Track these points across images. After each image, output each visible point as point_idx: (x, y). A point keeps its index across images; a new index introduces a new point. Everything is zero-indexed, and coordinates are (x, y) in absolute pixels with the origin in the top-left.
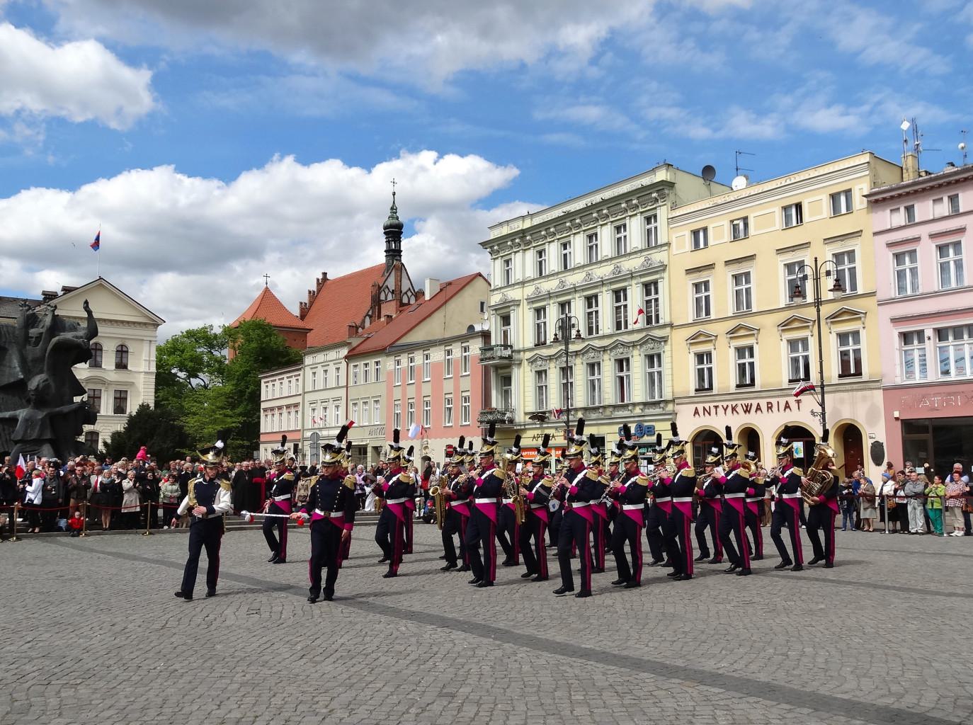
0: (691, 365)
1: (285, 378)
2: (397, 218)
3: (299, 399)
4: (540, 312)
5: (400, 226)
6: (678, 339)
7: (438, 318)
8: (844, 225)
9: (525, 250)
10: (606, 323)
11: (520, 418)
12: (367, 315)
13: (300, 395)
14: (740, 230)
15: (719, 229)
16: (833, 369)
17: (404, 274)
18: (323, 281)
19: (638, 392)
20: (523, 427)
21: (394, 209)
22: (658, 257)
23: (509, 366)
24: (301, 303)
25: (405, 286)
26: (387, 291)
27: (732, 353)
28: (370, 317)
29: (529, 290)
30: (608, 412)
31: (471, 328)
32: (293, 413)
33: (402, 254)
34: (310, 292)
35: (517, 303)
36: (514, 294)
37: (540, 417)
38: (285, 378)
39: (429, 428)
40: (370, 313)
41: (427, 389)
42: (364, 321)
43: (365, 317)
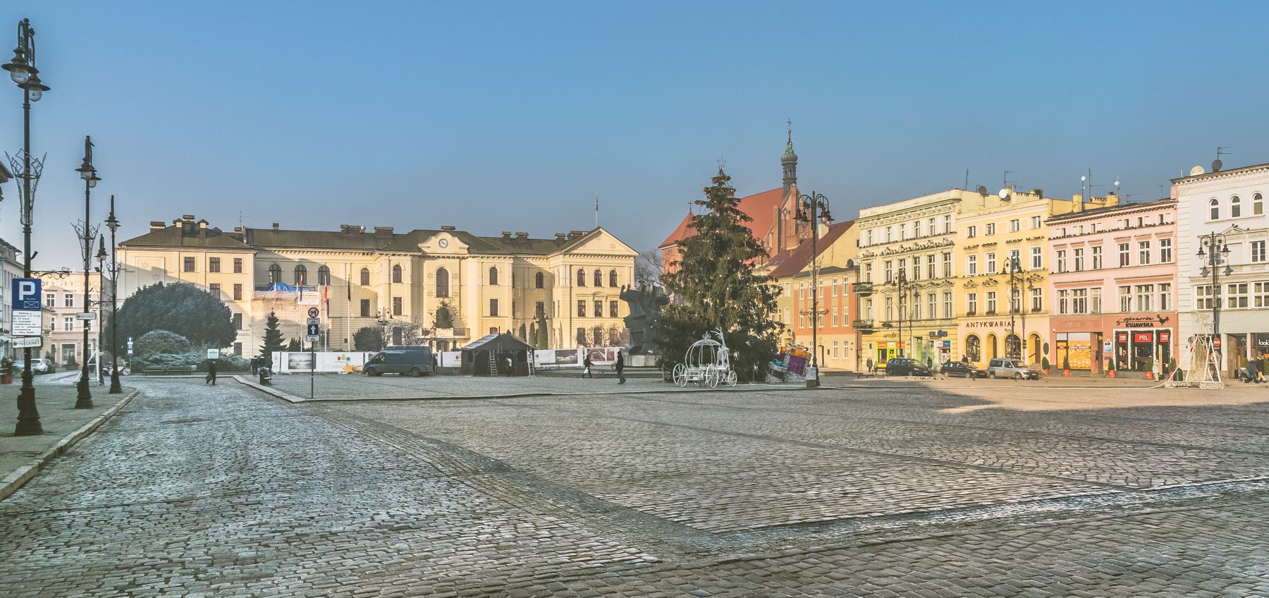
0: (967, 300)
5: (795, 158)
6: (958, 284)
7: (827, 252)
8: (1037, 233)
10: (924, 275)
11: (876, 324)
14: (991, 228)
15: (981, 231)
16: (1030, 306)
19: (940, 313)
22: (950, 238)
27: (986, 296)
29: (883, 249)
30: (923, 323)
31: (850, 262)
37: (887, 325)
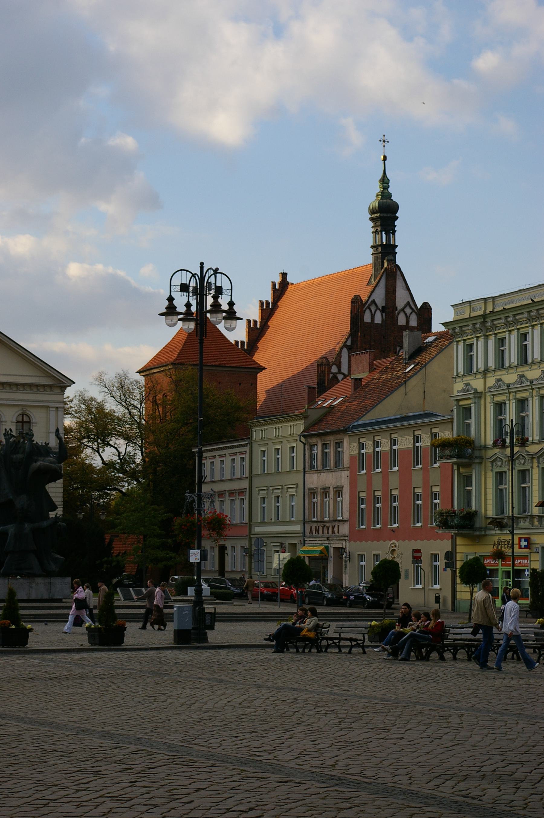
1: (228, 455)
2: (390, 195)
3: (245, 484)
4: (500, 407)
9: (488, 336)
12: (345, 345)
13: (246, 478)
17: (399, 283)
18: (281, 288)
20: (483, 533)
21: (385, 181)
23: (468, 466)
24: (249, 321)
25: (401, 301)
26: (373, 308)
28: (350, 349)
29: (491, 381)
32: (237, 502)
34: (262, 303)
35: (478, 395)
36: (478, 384)
37: (498, 523)
38: (228, 455)
40: (349, 343)
42: (339, 355)
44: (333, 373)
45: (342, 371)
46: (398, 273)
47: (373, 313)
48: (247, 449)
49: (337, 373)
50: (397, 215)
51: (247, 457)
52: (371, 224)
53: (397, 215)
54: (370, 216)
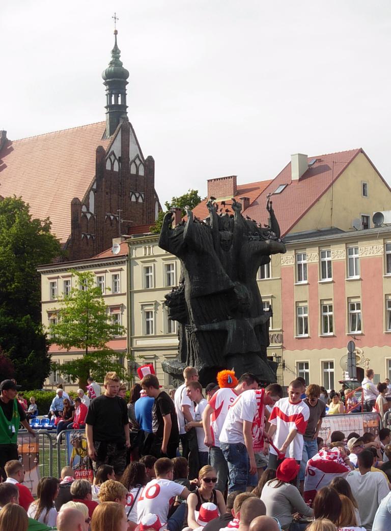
2: (121, 64)
3: (123, 300)
12: (91, 189)
21: (116, 52)
26: (113, 158)
28: (95, 191)
33: (128, 110)
39: (362, 334)
40: (95, 187)
41: (353, 290)
43: (90, 191)
44: (83, 213)
45: (90, 211)
46: (131, 129)
47: (113, 161)
48: (125, 267)
49: (86, 213)
50: (127, 80)
51: (123, 276)
52: (105, 88)
53: (127, 80)
54: (104, 81)
